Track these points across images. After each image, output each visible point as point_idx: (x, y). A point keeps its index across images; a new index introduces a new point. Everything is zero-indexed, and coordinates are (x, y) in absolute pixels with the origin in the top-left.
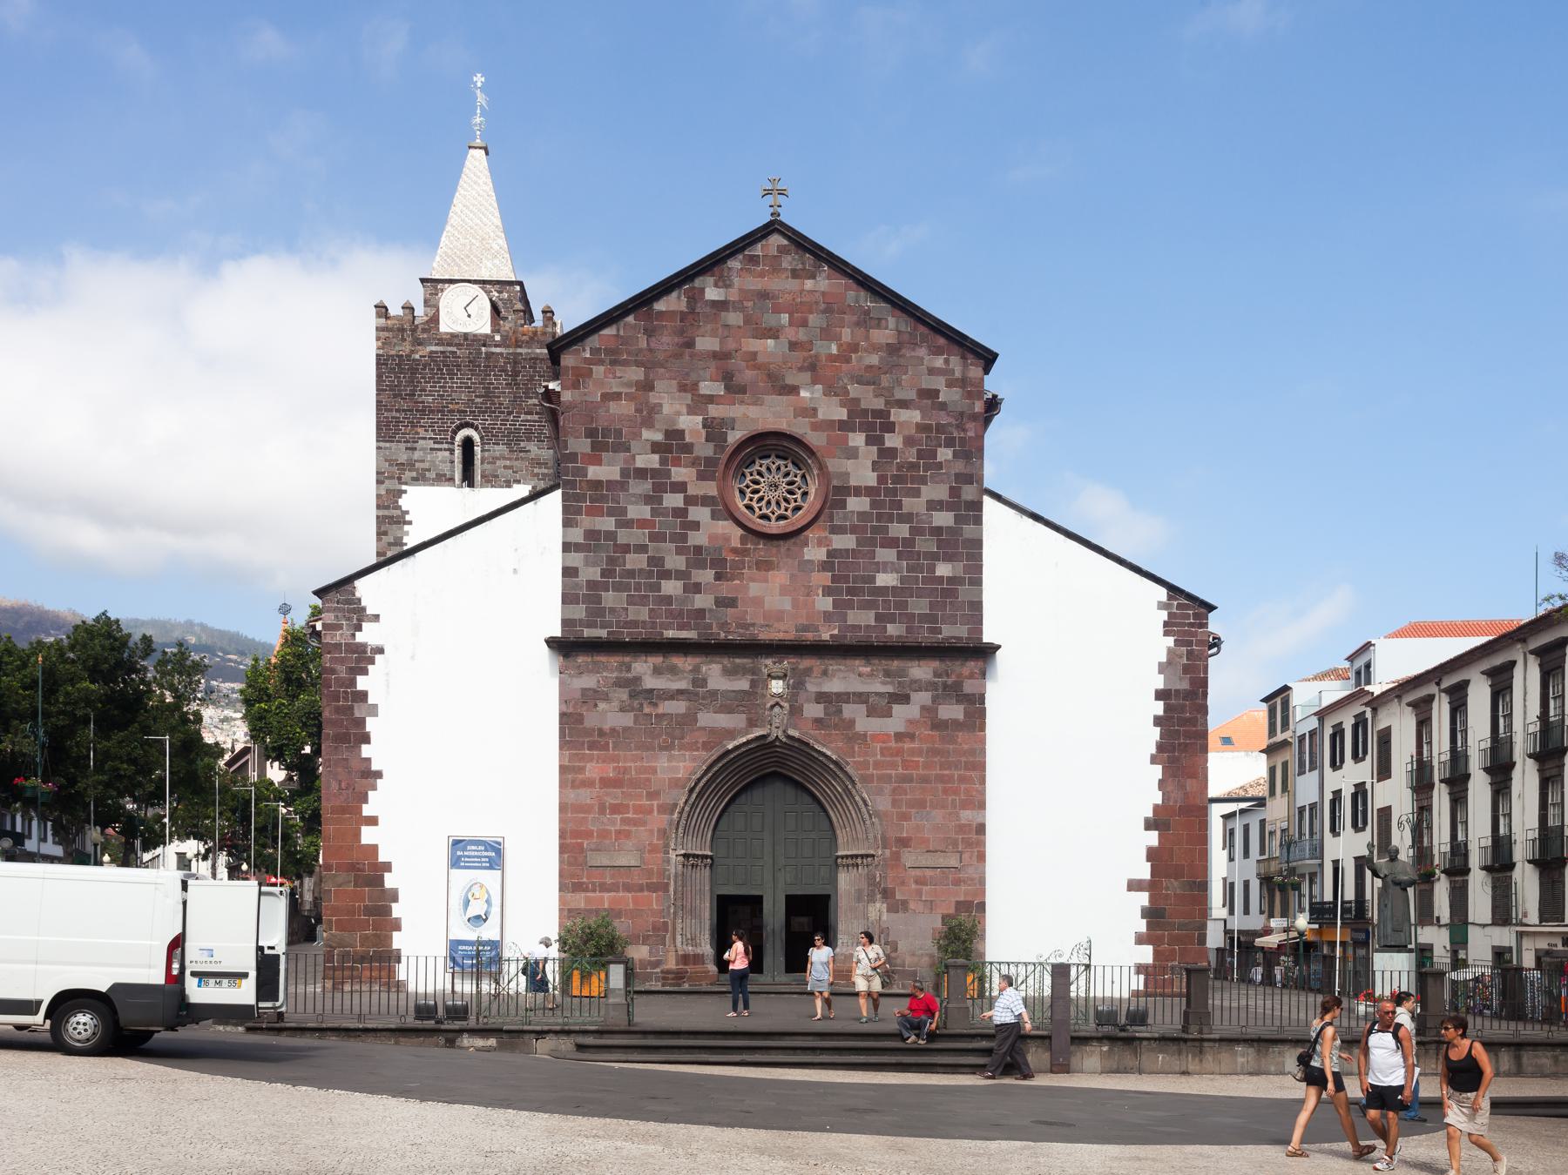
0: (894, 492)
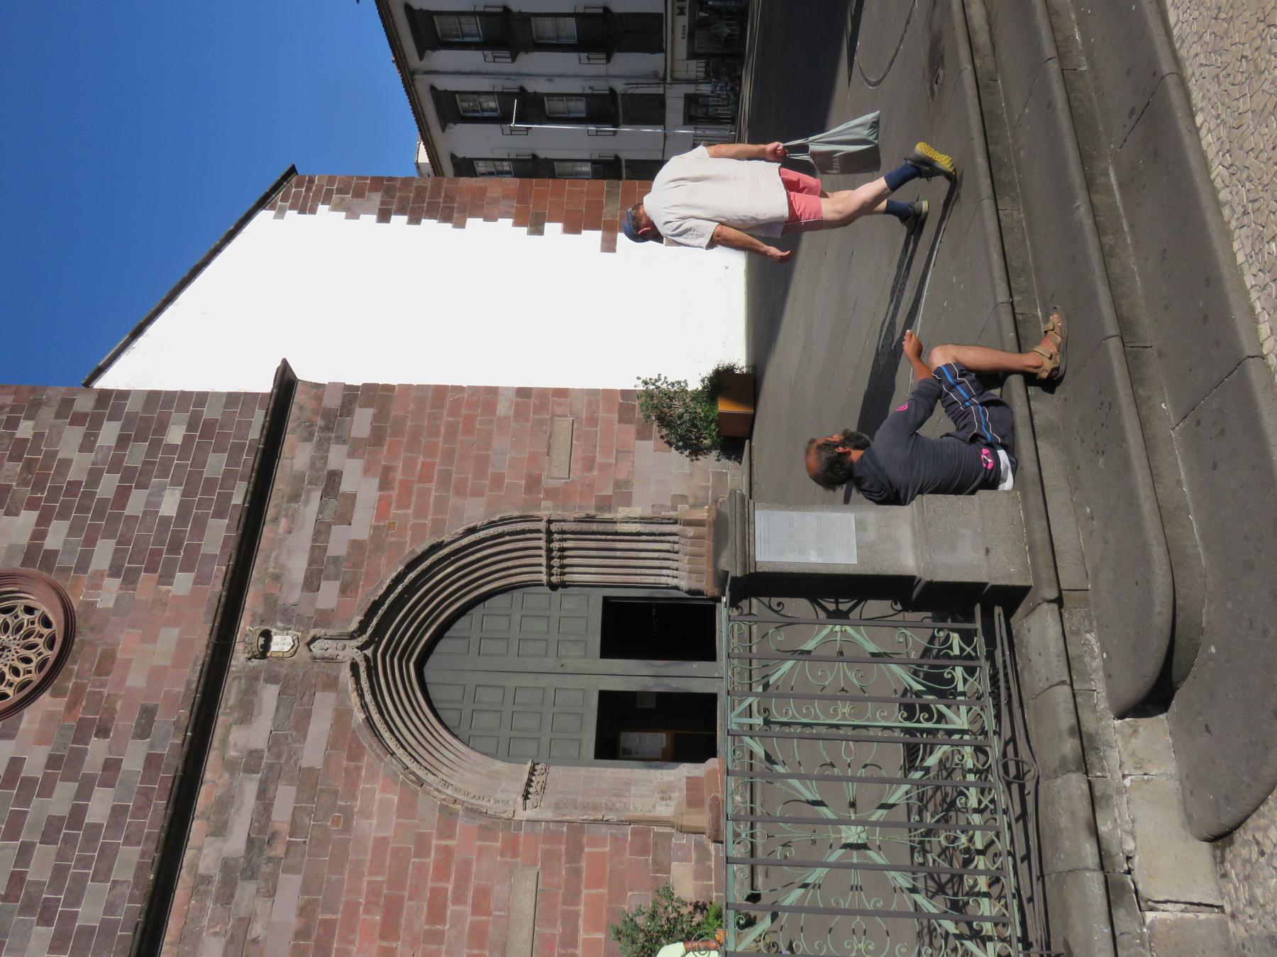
0: (55, 490)
